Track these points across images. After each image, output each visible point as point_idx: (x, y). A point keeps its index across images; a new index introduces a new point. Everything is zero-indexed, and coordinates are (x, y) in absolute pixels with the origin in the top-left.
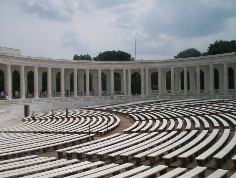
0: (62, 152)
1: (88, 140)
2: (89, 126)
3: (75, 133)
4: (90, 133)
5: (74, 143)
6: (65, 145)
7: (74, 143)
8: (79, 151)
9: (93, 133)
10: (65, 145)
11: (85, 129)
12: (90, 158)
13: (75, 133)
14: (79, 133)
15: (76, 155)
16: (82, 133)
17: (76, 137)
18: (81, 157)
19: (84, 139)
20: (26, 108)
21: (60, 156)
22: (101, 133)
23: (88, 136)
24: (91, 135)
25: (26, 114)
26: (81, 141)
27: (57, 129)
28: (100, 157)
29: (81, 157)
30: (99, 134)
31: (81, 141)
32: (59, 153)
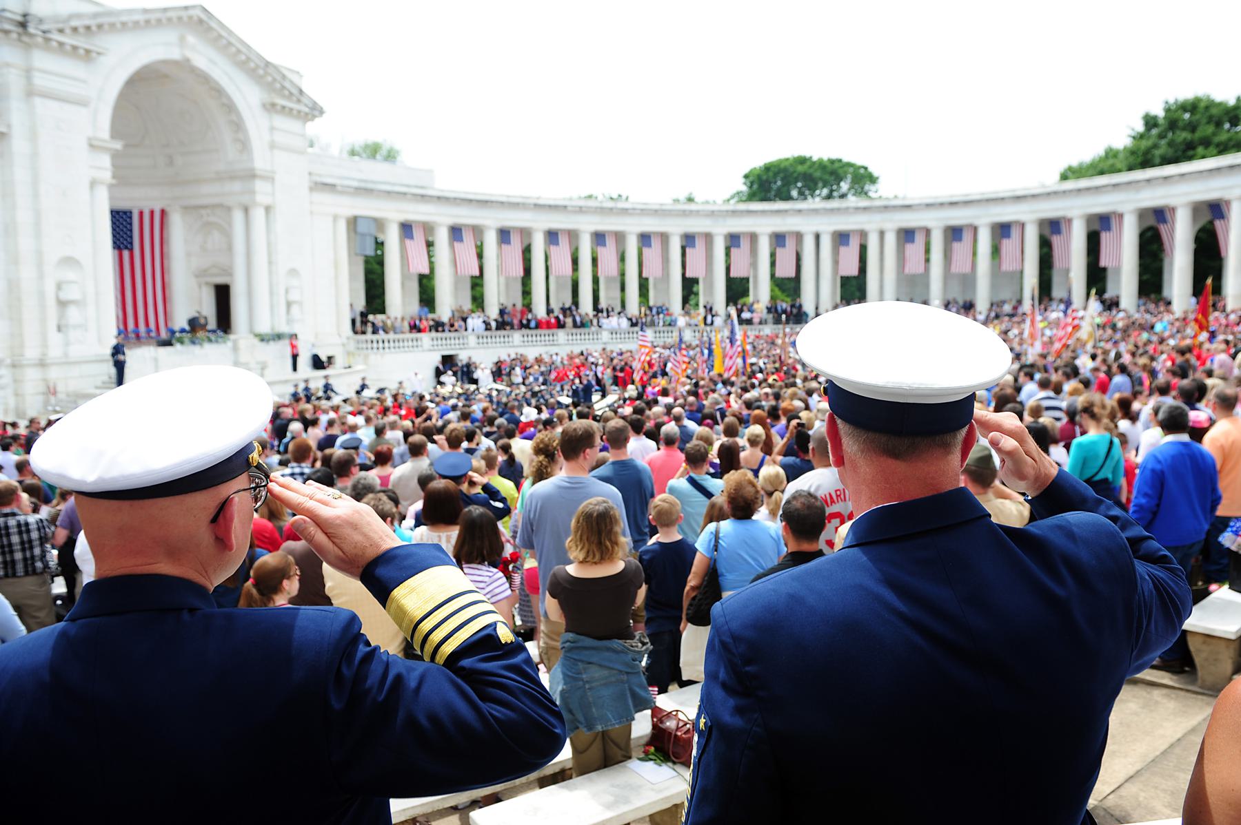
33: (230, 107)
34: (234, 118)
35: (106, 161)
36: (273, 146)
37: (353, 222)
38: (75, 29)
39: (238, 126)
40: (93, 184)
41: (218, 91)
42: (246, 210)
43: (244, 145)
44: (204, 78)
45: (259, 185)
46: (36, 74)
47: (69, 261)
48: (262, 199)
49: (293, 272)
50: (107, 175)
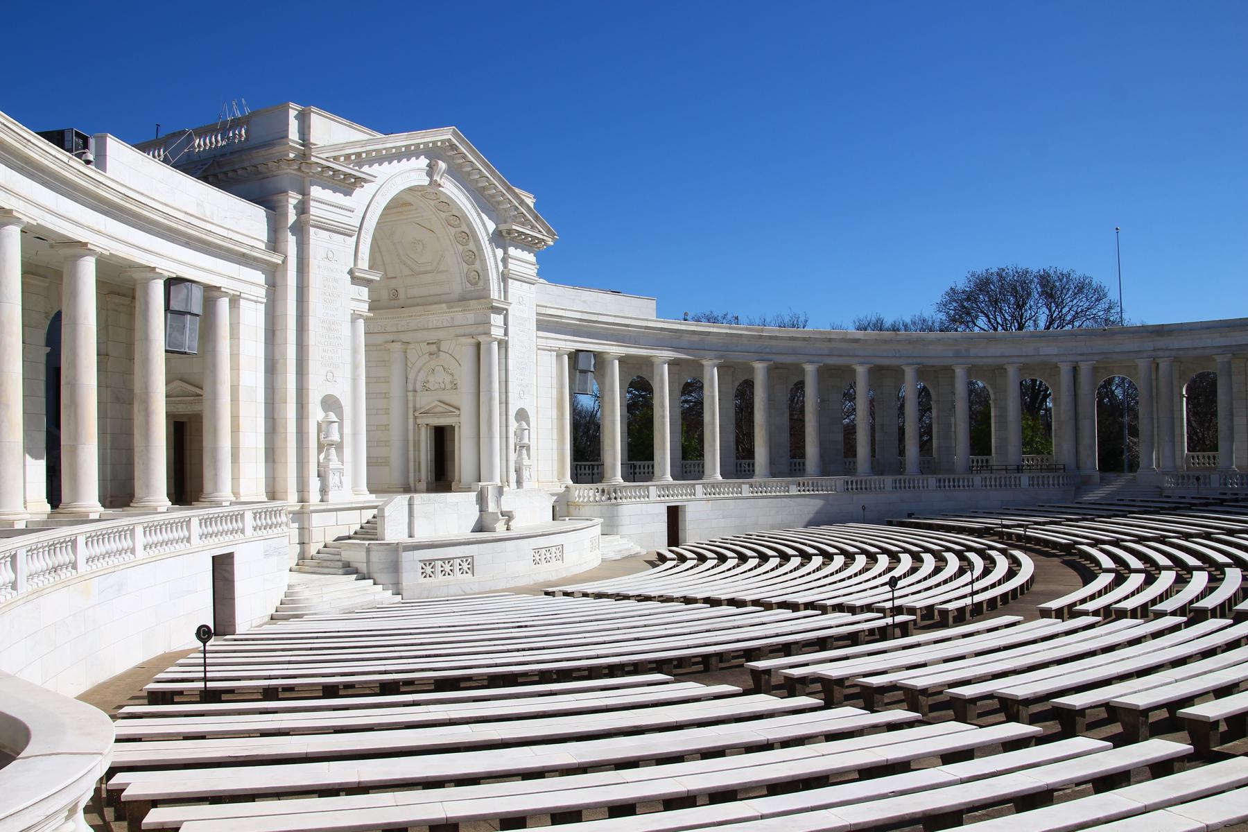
0: (768, 672)
1: (883, 634)
2: (893, 582)
3: (840, 608)
4: (898, 610)
5: (822, 644)
6: (787, 649)
7: (822, 644)
8: (834, 671)
9: (911, 611)
10: (787, 649)
11: (881, 595)
12: (870, 698)
13: (840, 608)
14: (852, 610)
15: (818, 686)
16: (868, 608)
17: (837, 623)
18: (833, 693)
19: (871, 631)
20: (674, 515)
21: (760, 683)
22: (944, 613)
23: (889, 620)
24: (899, 619)
25: (674, 538)
26: (853, 639)
27: (773, 593)
28: (912, 697)
29: (833, 693)
30: (933, 618)
31: (853, 639)
32: (756, 673)
33: (469, 235)
34: (472, 246)
35: (364, 292)
36: (504, 278)
37: (574, 356)
38: (348, 157)
39: (474, 256)
40: (355, 317)
41: (460, 217)
42: (479, 345)
43: (479, 278)
44: (447, 203)
45: (497, 319)
46: (312, 203)
47: (330, 403)
48: (497, 332)
49: (522, 415)
50: (364, 307)
